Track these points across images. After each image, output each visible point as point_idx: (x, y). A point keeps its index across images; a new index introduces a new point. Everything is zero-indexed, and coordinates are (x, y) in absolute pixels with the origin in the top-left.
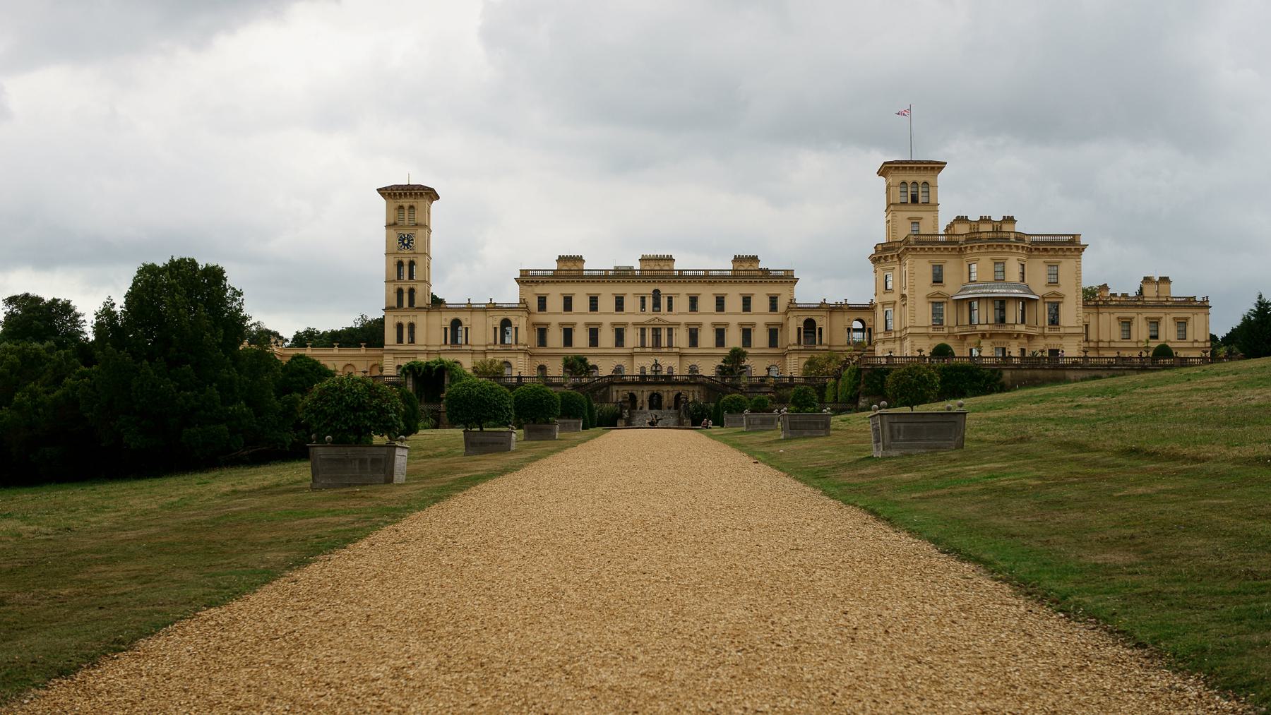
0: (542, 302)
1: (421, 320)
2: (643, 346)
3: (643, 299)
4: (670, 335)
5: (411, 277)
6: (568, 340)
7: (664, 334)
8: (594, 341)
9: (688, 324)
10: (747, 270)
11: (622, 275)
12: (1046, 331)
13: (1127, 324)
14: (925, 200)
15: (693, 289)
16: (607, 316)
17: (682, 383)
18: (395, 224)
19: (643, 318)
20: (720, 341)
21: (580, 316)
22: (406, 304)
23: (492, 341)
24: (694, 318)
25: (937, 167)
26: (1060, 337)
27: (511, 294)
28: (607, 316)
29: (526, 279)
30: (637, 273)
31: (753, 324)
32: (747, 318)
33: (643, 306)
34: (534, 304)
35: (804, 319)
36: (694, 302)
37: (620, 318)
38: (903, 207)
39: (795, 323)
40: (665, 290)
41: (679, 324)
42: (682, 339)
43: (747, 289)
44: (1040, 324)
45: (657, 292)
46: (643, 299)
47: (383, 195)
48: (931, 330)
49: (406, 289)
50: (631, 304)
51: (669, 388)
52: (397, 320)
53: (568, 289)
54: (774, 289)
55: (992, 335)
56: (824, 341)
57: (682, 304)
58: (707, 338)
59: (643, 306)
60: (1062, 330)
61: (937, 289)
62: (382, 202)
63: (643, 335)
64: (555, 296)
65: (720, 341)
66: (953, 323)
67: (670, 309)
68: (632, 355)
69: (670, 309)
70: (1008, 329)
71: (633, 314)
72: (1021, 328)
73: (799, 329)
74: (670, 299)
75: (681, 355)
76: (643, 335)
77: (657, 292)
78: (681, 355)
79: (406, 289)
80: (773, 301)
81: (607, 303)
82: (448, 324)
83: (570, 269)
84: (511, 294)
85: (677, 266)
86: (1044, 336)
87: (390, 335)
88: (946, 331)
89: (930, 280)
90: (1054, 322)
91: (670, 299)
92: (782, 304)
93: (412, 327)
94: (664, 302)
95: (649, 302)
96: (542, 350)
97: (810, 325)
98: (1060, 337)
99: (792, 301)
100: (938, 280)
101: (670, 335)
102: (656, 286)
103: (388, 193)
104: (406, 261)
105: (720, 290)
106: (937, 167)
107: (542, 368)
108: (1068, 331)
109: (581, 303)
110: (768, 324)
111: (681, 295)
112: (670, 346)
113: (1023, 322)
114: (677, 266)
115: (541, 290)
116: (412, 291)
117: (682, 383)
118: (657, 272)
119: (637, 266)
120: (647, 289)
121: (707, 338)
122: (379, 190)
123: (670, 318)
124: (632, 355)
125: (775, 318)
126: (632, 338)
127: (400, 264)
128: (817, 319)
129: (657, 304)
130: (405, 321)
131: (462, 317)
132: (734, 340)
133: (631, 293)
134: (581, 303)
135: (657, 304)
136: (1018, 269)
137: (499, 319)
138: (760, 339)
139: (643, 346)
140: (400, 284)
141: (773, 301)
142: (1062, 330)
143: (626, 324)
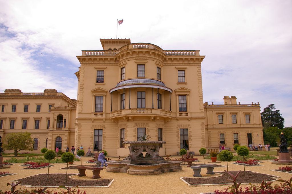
6: (24, 127)
8: (37, 127)
9: (10, 118)
12: (178, 115)
13: (221, 115)
24: (13, 115)
26: (188, 119)
32: (38, 115)
35: (57, 115)
41: (6, 118)
44: (173, 110)
48: (92, 116)
55: (134, 118)
56: (67, 126)
60: (189, 115)
66: (109, 111)
70: (147, 113)
72: (156, 112)
86: (177, 119)
88: (104, 116)
89: (95, 80)
90: (183, 110)
97: (60, 118)
98: (188, 119)
100: (100, 81)
108: (194, 115)
111: (20, 104)
113: (160, 107)
136: (155, 70)
142: (189, 115)
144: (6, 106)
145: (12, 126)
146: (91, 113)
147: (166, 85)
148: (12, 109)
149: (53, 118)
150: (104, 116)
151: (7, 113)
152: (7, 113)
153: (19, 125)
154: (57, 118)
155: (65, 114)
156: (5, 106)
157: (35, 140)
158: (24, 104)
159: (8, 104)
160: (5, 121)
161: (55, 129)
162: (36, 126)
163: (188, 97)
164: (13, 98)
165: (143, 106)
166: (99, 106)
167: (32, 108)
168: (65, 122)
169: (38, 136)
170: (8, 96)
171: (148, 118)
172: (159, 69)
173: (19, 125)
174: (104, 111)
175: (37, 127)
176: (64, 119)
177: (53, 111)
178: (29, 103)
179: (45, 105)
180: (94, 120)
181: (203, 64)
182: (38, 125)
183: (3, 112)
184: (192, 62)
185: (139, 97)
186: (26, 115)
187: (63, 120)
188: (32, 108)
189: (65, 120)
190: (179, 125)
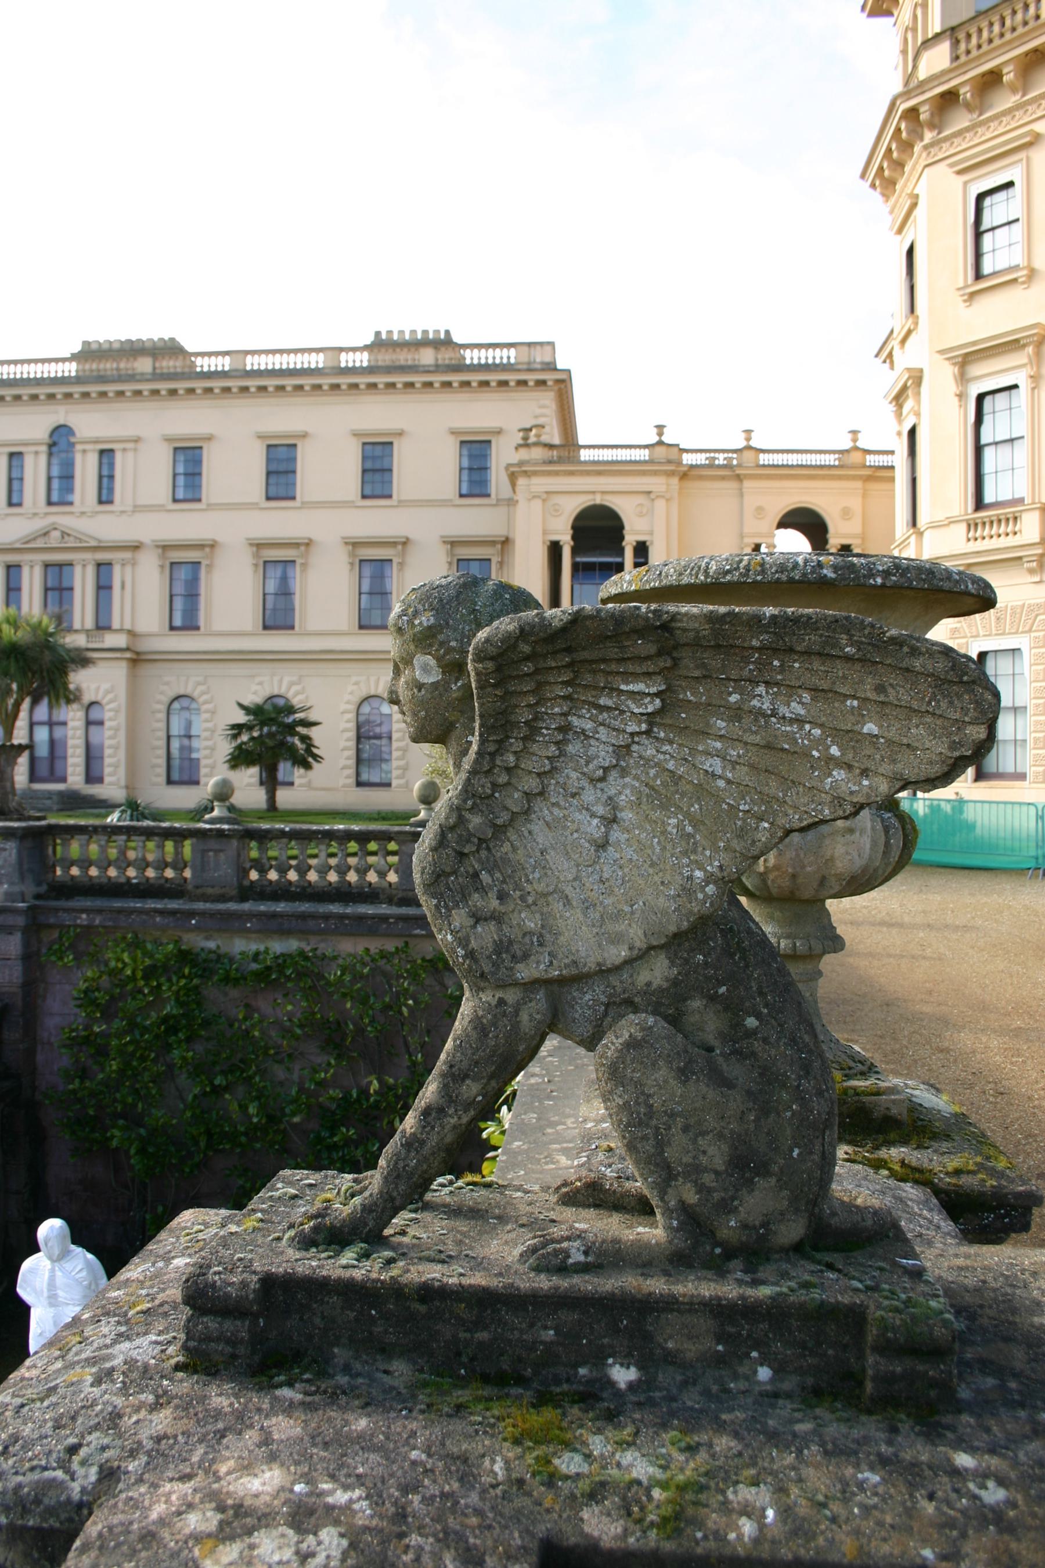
3: (15, 457)
4: (103, 588)
7: (83, 582)
9: (165, 548)
24: (187, 525)
35: (572, 507)
36: (189, 462)
40: (91, 424)
41: (136, 547)
43: (378, 414)
45: (60, 440)
46: (15, 457)
57: (147, 475)
67: (105, 497)
69: (105, 497)
73: (555, 549)
74: (106, 455)
77: (60, 440)
91: (106, 455)
94: (86, 470)
95: (36, 471)
101: (103, 588)
144: (130, 455)
145: (186, 608)
148: (175, 475)
149: (545, 532)
152: (137, 509)
153: (232, 598)
154: (573, 538)
155: (641, 499)
156: (118, 457)
157: (366, 709)
158: (261, 437)
159: (137, 440)
160: (128, 569)
162: (270, 605)
164: (173, 392)
167: (329, 468)
169: (199, 684)
170: (132, 377)
173: (232, 598)
175: (278, 615)
177: (535, 480)
179: (427, 434)
182: (285, 592)
183: (110, 502)
186: (280, 523)
187: (621, 552)
188: (329, 468)
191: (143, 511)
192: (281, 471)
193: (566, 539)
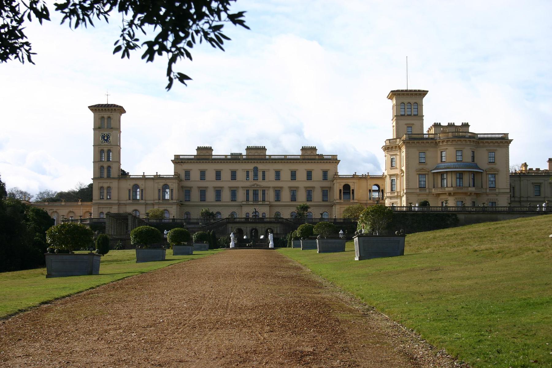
0: (187, 173)
1: (114, 184)
2: (248, 200)
3: (248, 172)
4: (264, 194)
5: (108, 159)
9: (274, 188)
10: (309, 155)
11: (235, 158)
12: (488, 191)
14: (416, 113)
15: (278, 167)
16: (226, 183)
17: (270, 222)
18: (99, 128)
19: (248, 184)
20: (293, 198)
21: (210, 182)
22: (105, 175)
23: (157, 197)
25: (423, 93)
27: (169, 170)
28: (226, 183)
29: (178, 161)
30: (244, 157)
31: (314, 188)
32: (309, 184)
33: (248, 176)
34: (183, 176)
35: (343, 184)
37: (234, 184)
38: (402, 118)
39: (338, 186)
40: (261, 167)
41: (269, 187)
42: (271, 196)
43: (309, 166)
45: (256, 170)
46: (248, 172)
47: (92, 110)
48: (418, 191)
49: (105, 166)
50: (241, 175)
51: (263, 225)
52: (101, 185)
53: (203, 166)
54: (326, 167)
57: (270, 176)
58: (286, 196)
59: (248, 176)
60: (497, 191)
61: (422, 166)
62: (91, 115)
63: (248, 194)
64: (195, 170)
65: (293, 198)
67: (264, 179)
68: (241, 206)
69: (264, 179)
70: (464, 190)
71: (241, 181)
72: (472, 189)
73: (340, 190)
74: (264, 173)
75: (271, 206)
76: (248, 194)
77: (256, 170)
78: (271, 206)
79: (105, 166)
80: (325, 173)
81: (226, 175)
82: (131, 187)
83: (204, 154)
84: (169, 170)
85: (268, 153)
86: (487, 195)
87: (96, 194)
91: (264, 173)
92: (330, 175)
93: (109, 188)
94: (260, 175)
95: (251, 174)
96: (187, 203)
99: (336, 174)
101: (264, 194)
102: (256, 165)
103: (95, 108)
104: (106, 149)
105: (294, 167)
106: (423, 93)
107: (188, 214)
109: (210, 175)
110: (322, 188)
111: (271, 168)
112: (264, 200)
113: (474, 186)
114: (268, 153)
115: (186, 167)
116: (109, 167)
117: (270, 222)
118: (256, 155)
119: (244, 153)
120: (250, 167)
121: (286, 196)
122: (89, 107)
123: (264, 184)
124: (241, 206)
125: (326, 184)
126: (241, 196)
127: (102, 151)
128: (351, 184)
129: (256, 175)
130: (105, 185)
131: (140, 183)
132: (302, 198)
133: (240, 168)
134: (210, 175)
135: (256, 175)
136: (470, 154)
137: (162, 184)
138: (317, 196)
139: (248, 200)
140: (102, 164)
141: (325, 173)
143: (239, 187)
146: (416, 189)
147: (479, 166)
150: (427, 191)
151: (269, 181)
152: (269, 181)
161: (342, 201)
163: (497, 176)
165: (461, 184)
166: (422, 183)
167: (301, 175)
168: (353, 193)
171: (466, 194)
172: (473, 152)
174: (427, 187)
176: (351, 189)
178: (296, 168)
180: (419, 195)
181: (511, 146)
184: (501, 144)
185: (458, 177)
189: (353, 190)
190: (488, 199)
191: (270, 182)
192: (293, 175)
193: (342, 189)
